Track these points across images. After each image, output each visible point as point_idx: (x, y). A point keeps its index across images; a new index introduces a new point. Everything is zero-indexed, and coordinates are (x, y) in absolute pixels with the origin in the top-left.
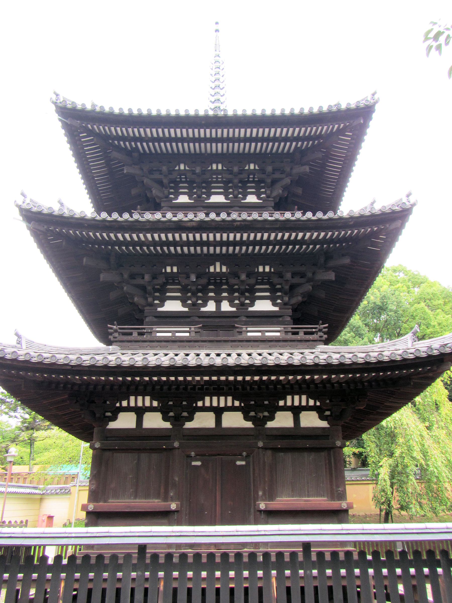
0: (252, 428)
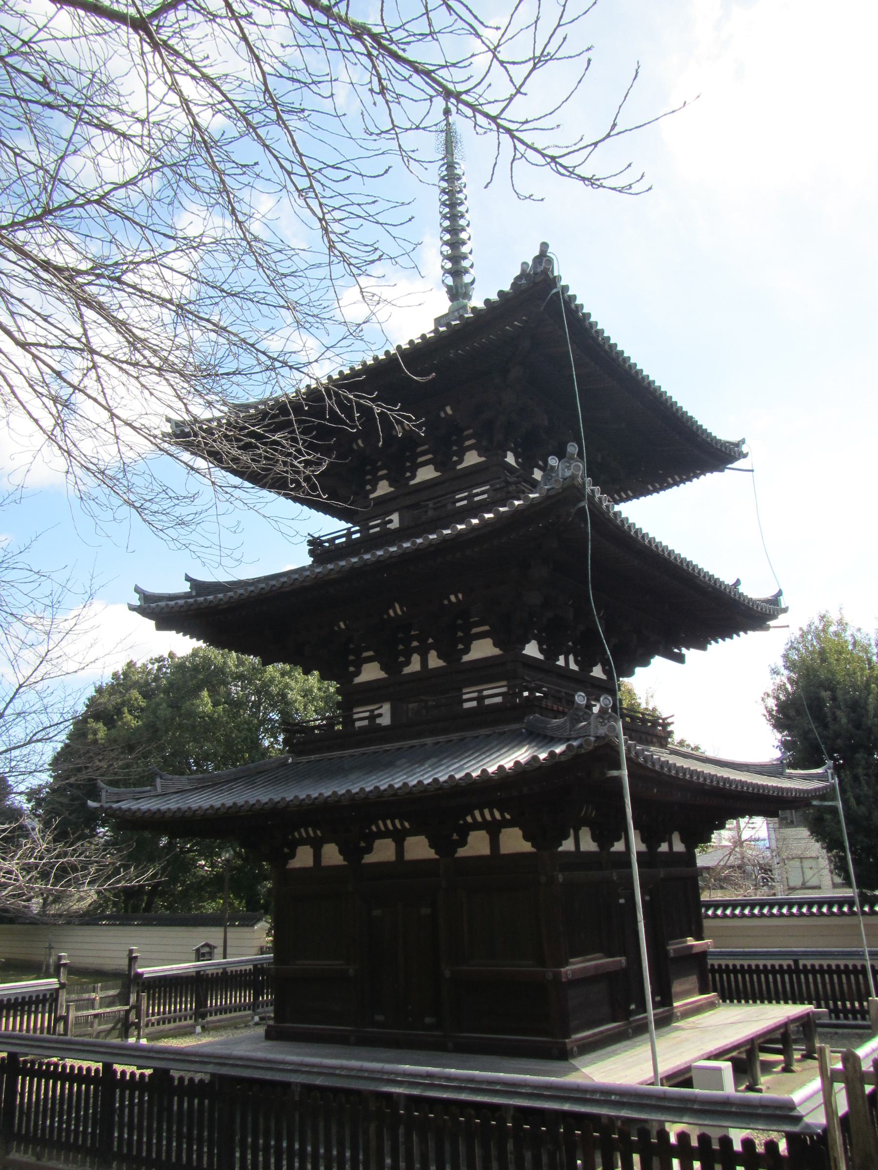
0: (436, 860)
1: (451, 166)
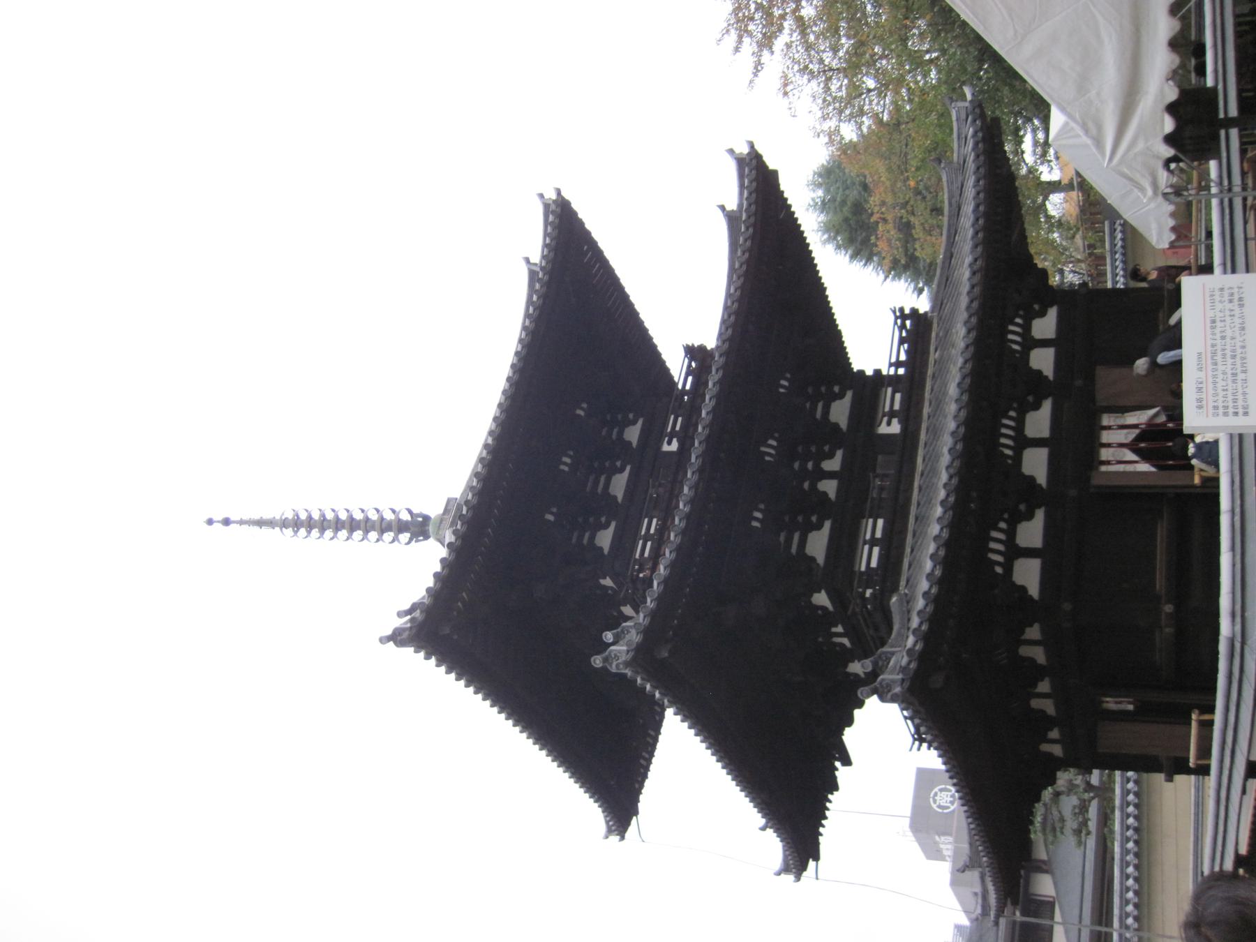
1: (284, 524)
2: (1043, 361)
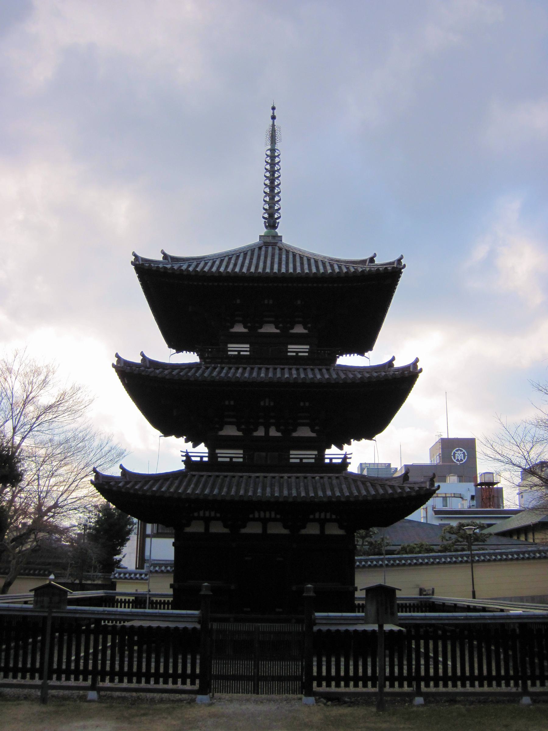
1: (273, 150)
2: (312, 530)
